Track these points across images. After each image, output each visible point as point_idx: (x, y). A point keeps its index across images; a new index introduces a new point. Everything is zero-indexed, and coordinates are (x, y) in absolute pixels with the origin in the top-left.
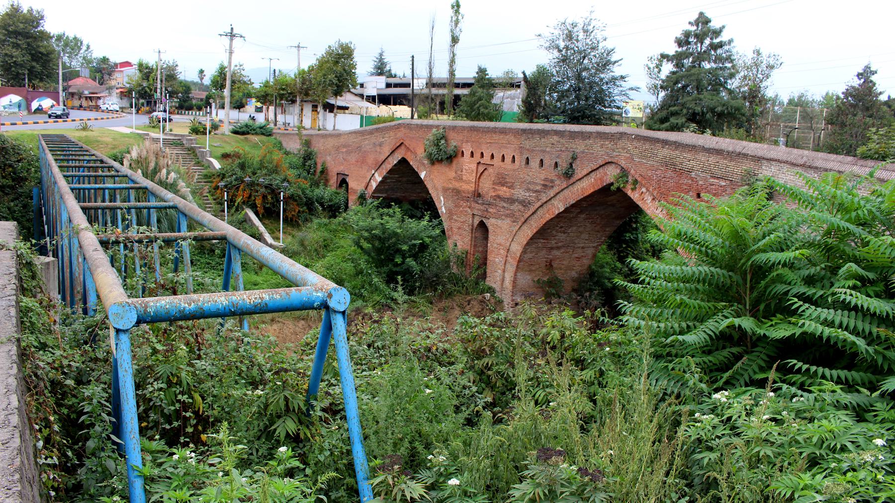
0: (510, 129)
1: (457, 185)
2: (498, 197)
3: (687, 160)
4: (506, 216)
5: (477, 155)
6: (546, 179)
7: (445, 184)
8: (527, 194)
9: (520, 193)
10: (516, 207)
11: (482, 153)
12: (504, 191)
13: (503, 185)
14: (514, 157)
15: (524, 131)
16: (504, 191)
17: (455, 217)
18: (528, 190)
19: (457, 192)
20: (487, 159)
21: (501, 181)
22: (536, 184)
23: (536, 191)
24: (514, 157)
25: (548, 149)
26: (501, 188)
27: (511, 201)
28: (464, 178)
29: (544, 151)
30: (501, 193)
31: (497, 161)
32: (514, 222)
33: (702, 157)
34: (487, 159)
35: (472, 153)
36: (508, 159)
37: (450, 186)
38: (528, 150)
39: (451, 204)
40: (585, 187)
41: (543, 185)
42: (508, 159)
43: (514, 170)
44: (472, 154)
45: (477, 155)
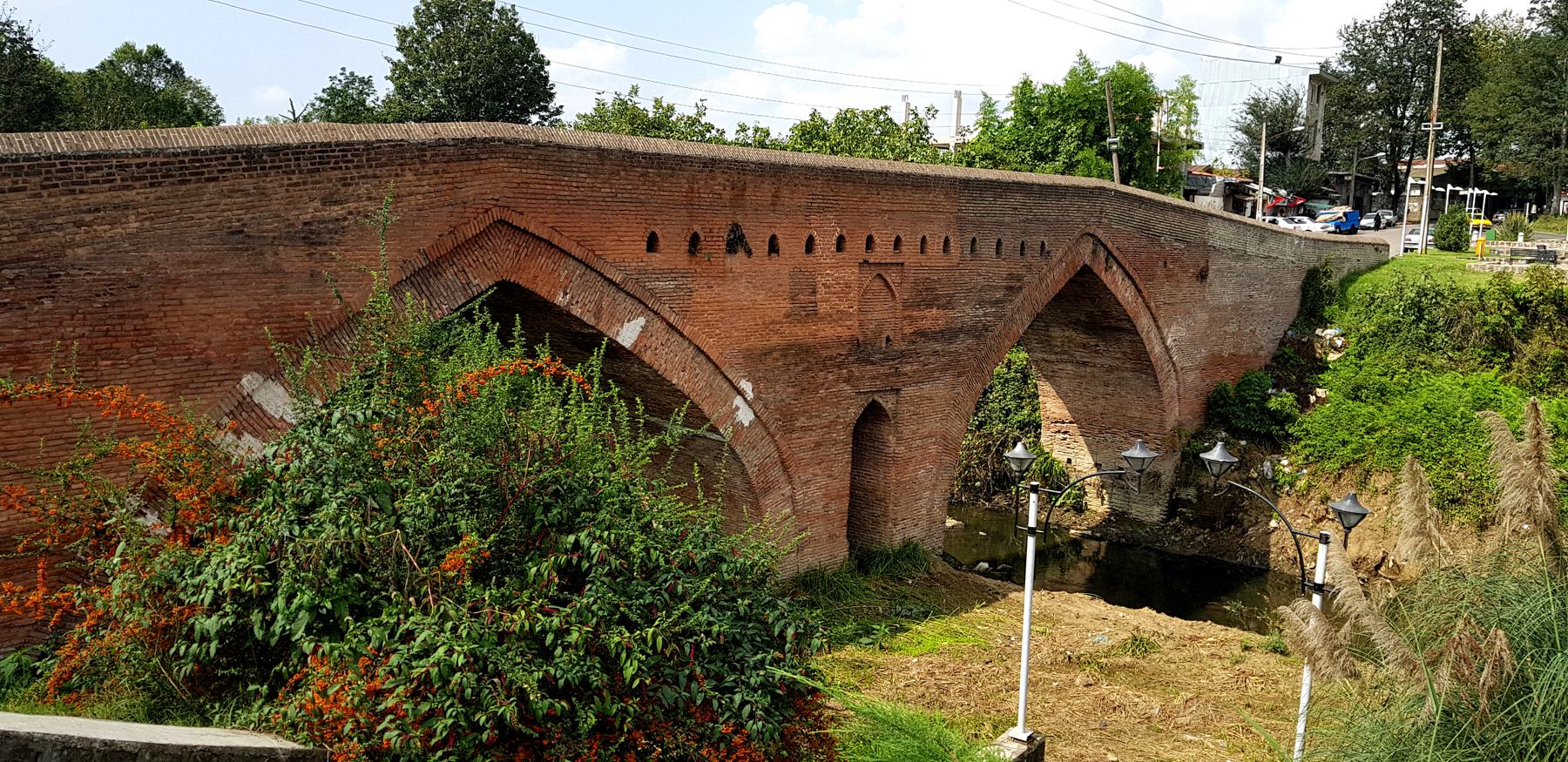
0: (937, 178)
1: (800, 333)
2: (921, 334)
3: (1162, 224)
4: (944, 370)
5: (856, 246)
6: (1011, 276)
7: (756, 342)
8: (980, 312)
9: (967, 313)
10: (960, 345)
11: (811, 240)
12: (932, 318)
13: (930, 306)
14: (947, 240)
15: (966, 183)
16: (932, 318)
17: (801, 421)
18: (982, 303)
19: (801, 353)
20: (884, 250)
21: (927, 296)
22: (995, 288)
23: (998, 302)
24: (947, 240)
25: (1007, 219)
26: (926, 312)
27: (949, 334)
28: (823, 308)
29: (1002, 224)
30: (926, 324)
31: (909, 253)
32: (960, 375)
33: (1170, 216)
34: (884, 250)
35: (841, 239)
36: (935, 246)
37: (775, 340)
38: (972, 222)
39: (782, 392)
40: (1056, 277)
41: (1010, 288)
42: (935, 246)
43: (951, 268)
44: (840, 244)
45: (856, 246)
